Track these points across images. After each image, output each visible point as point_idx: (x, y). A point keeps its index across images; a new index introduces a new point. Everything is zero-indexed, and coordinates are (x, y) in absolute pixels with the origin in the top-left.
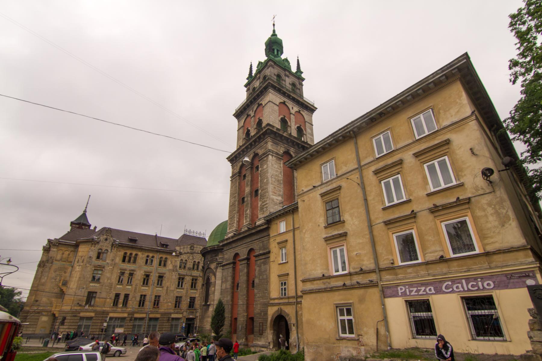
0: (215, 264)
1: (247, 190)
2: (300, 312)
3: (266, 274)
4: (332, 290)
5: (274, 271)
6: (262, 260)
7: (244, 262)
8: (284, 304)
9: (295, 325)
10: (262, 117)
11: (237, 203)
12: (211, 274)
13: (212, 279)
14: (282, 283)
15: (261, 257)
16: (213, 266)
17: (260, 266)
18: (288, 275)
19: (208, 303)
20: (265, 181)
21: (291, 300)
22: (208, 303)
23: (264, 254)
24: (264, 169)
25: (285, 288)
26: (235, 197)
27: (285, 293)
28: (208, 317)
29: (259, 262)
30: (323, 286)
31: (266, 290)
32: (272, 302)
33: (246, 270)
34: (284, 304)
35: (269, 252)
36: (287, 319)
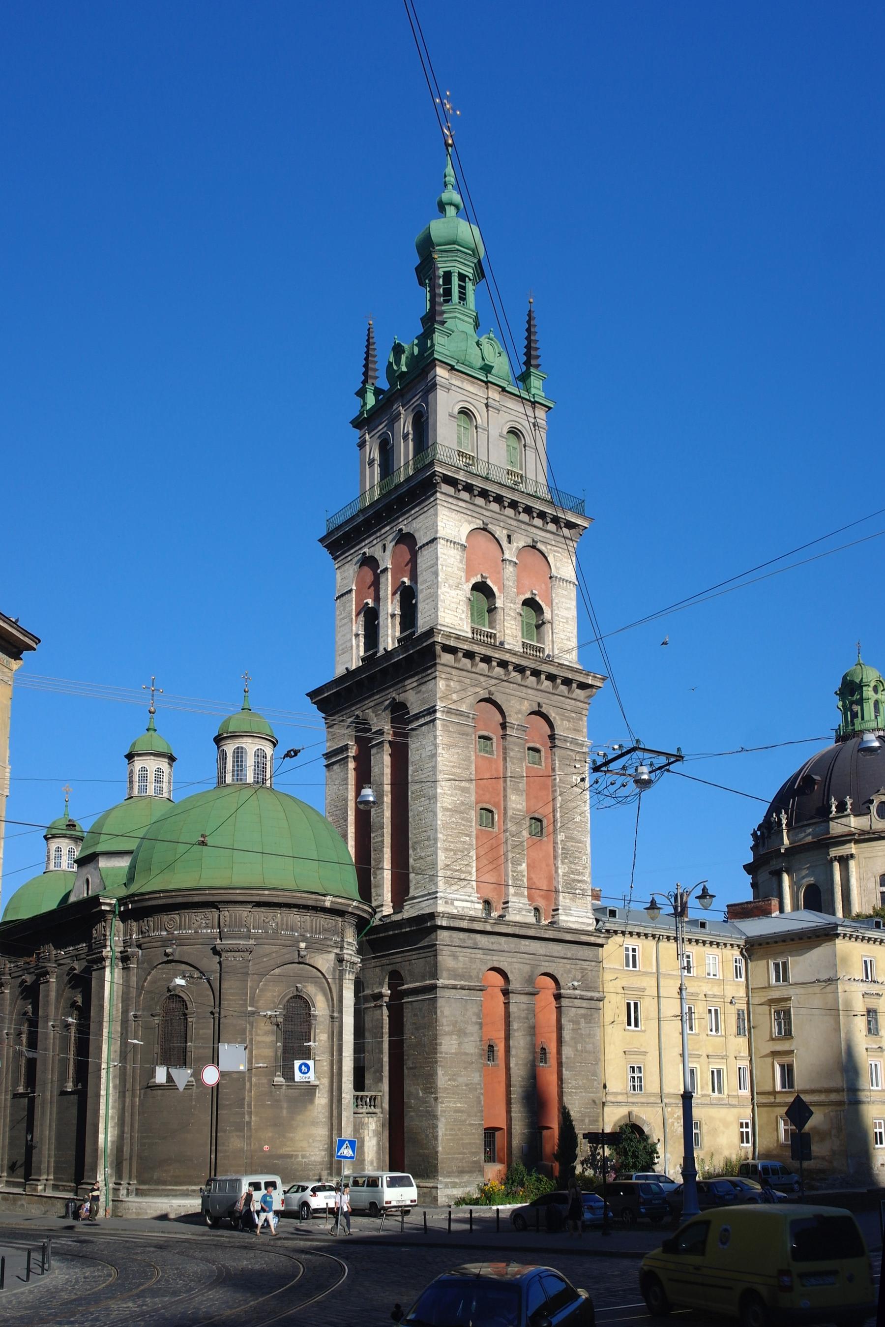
0: (332, 957)
1: (517, 803)
2: (670, 1120)
3: (593, 1044)
5: (616, 1041)
6: (583, 1011)
9: (662, 1139)
10: (551, 604)
11: (473, 813)
15: (577, 1002)
17: (576, 1022)
23: (591, 999)
25: (640, 1078)
27: (641, 1086)
31: (595, 1074)
36: (646, 1129)
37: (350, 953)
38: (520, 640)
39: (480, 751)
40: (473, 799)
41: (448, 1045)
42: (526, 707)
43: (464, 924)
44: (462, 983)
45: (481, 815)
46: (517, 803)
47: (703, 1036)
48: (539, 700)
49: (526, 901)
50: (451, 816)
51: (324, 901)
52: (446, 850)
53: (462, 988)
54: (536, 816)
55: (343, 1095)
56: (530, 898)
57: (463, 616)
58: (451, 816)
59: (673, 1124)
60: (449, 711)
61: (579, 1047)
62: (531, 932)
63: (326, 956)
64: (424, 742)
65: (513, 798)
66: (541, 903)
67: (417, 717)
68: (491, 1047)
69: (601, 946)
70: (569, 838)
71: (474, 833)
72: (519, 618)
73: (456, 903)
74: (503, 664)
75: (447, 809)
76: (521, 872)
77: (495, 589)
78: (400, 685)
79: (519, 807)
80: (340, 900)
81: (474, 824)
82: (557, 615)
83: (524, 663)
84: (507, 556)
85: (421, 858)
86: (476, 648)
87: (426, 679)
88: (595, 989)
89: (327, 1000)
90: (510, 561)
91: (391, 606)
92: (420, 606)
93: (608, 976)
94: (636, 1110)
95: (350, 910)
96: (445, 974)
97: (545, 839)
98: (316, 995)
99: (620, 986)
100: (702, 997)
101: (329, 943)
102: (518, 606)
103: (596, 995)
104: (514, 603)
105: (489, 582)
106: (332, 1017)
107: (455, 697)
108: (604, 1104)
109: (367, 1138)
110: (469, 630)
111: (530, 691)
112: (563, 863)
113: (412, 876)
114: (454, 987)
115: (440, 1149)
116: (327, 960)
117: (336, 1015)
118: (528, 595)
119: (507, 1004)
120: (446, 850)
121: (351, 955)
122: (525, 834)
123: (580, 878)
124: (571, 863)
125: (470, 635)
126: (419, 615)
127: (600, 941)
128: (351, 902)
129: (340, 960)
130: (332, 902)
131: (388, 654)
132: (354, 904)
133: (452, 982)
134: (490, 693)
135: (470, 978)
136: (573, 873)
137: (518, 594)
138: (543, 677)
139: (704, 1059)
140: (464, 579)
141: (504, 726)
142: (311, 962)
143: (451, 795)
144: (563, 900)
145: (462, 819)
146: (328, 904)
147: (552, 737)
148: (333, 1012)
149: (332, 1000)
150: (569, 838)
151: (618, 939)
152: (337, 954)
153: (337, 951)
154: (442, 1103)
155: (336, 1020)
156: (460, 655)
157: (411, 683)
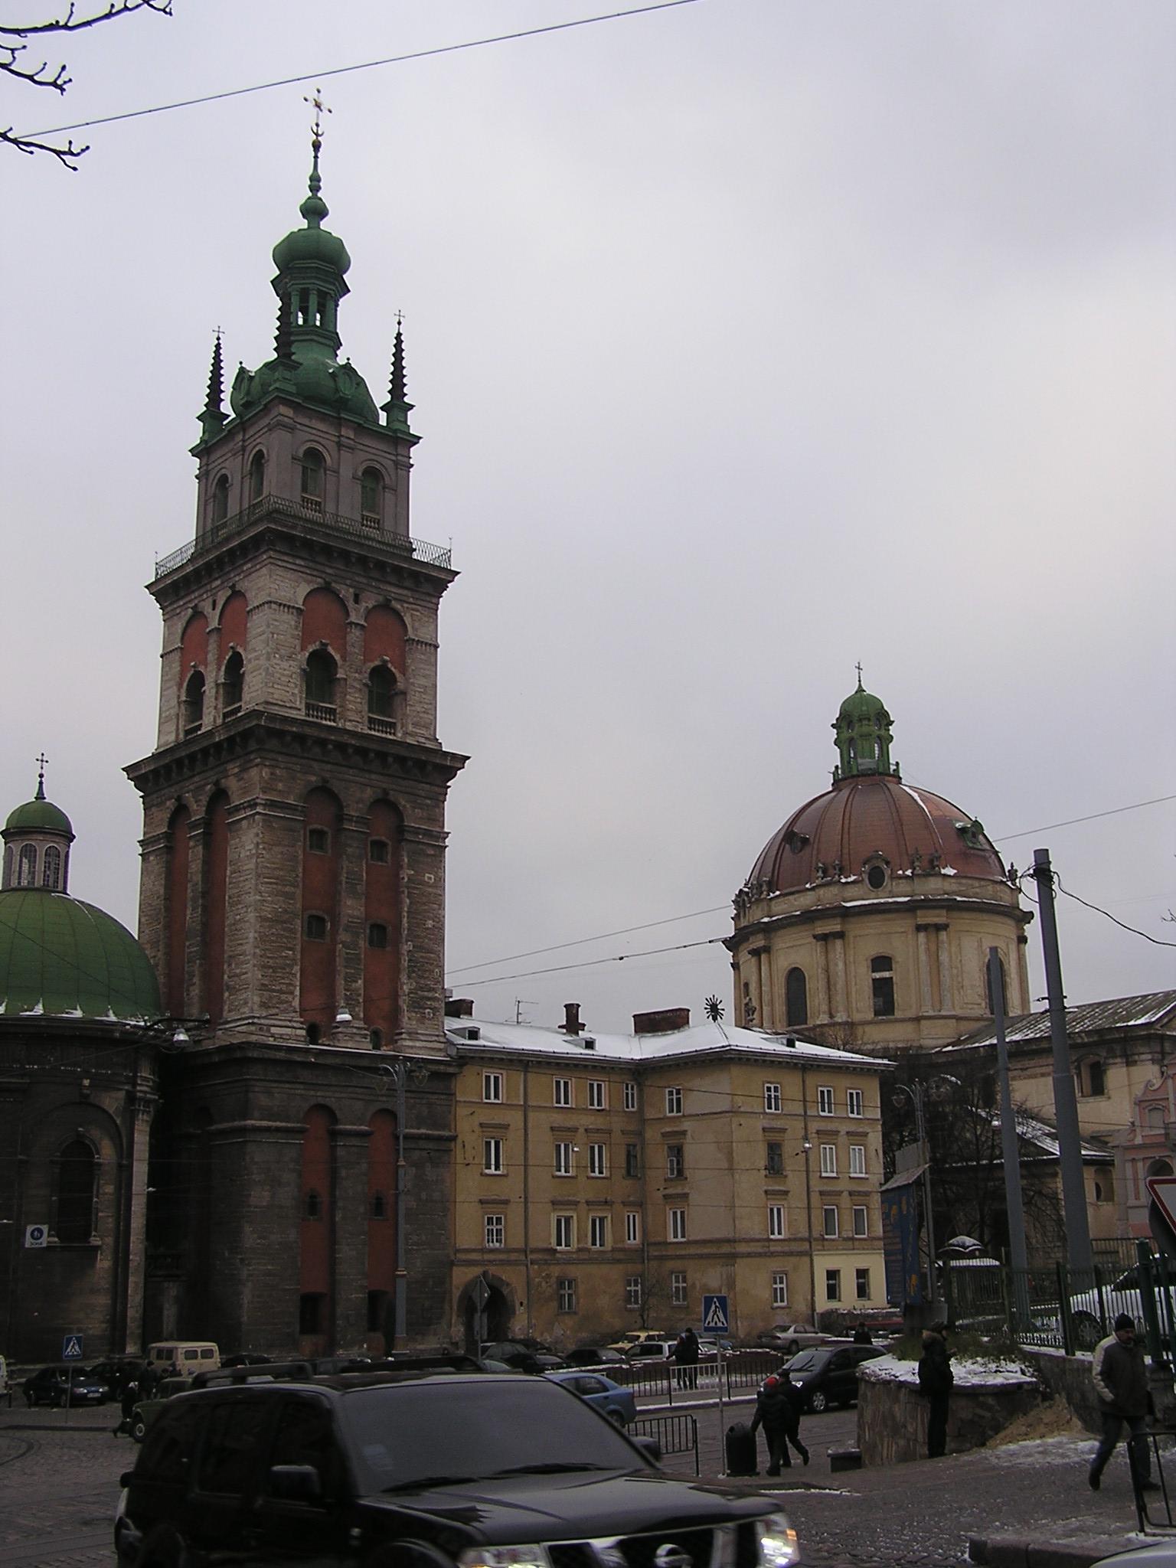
0: (122, 1095)
4: (772, 1254)
5: (468, 1186)
7: (355, 1141)
8: (503, 1263)
9: (525, 1302)
12: (95, 1133)
13: (107, 1153)
14: (490, 1221)
15: (422, 1144)
18: (506, 1202)
19: (95, 1241)
20: (430, 923)
21: (513, 1256)
22: (95, 1241)
23: (440, 1138)
24: (423, 883)
25: (499, 1232)
26: (286, 895)
29: (416, 1155)
30: (760, 1250)
32: (460, 1256)
33: (364, 1166)
34: (503, 1263)
35: (454, 1138)
37: (143, 1089)
38: (366, 714)
39: (311, 847)
40: (299, 906)
41: (259, 1196)
42: (369, 794)
43: (281, 1055)
44: (278, 1124)
45: (309, 923)
46: (352, 908)
47: (582, 1179)
48: (384, 786)
49: (361, 1024)
50: (270, 927)
51: (112, 1031)
52: (264, 967)
53: (278, 1129)
54: (379, 922)
56: (366, 1020)
57: (296, 691)
58: (270, 927)
59: (540, 1284)
60: (271, 804)
61: (424, 1196)
62: (365, 1063)
63: (114, 1094)
64: (244, 838)
65: (349, 903)
66: (381, 1026)
67: (237, 809)
68: (313, 1197)
69: (453, 1075)
70: (419, 948)
71: (298, 948)
72: (366, 690)
73: (273, 1030)
74: (341, 747)
75: (266, 919)
76: (358, 989)
77: (337, 657)
78: (221, 768)
79: (356, 913)
81: (299, 935)
82: (413, 684)
83: (365, 744)
84: (353, 618)
85: (236, 975)
86: (308, 731)
88: (444, 1127)
90: (357, 625)
91: (214, 676)
92: (247, 678)
93: (462, 1111)
94: (493, 1270)
96: (256, 1114)
97: (388, 949)
99: (477, 1123)
100: (581, 1130)
102: (365, 678)
103: (446, 1133)
104: (360, 673)
105: (330, 649)
106: (120, 1166)
107: (280, 786)
108: (452, 1264)
109: (167, 1306)
110: (303, 707)
111: (373, 776)
112: (409, 977)
113: (226, 994)
114: (268, 1129)
115: (245, 1319)
118: (377, 663)
119: (333, 1148)
120: (264, 967)
121: (145, 1092)
122: (362, 943)
123: (430, 995)
124: (420, 977)
125: (301, 715)
126: (246, 688)
127: (451, 1070)
129: (131, 1098)
131: (210, 733)
133: (265, 1123)
134: (325, 781)
135: (287, 1119)
136: (422, 989)
137: (365, 661)
138: (390, 759)
139: (583, 1207)
140: (298, 648)
141: (340, 818)
143: (272, 902)
144: (408, 1021)
145: (284, 930)
147: (400, 831)
149: (121, 1145)
150: (419, 948)
151: (476, 1069)
152: (128, 1091)
154: (249, 1265)
155: (125, 1170)
156: (289, 738)
157: (233, 768)
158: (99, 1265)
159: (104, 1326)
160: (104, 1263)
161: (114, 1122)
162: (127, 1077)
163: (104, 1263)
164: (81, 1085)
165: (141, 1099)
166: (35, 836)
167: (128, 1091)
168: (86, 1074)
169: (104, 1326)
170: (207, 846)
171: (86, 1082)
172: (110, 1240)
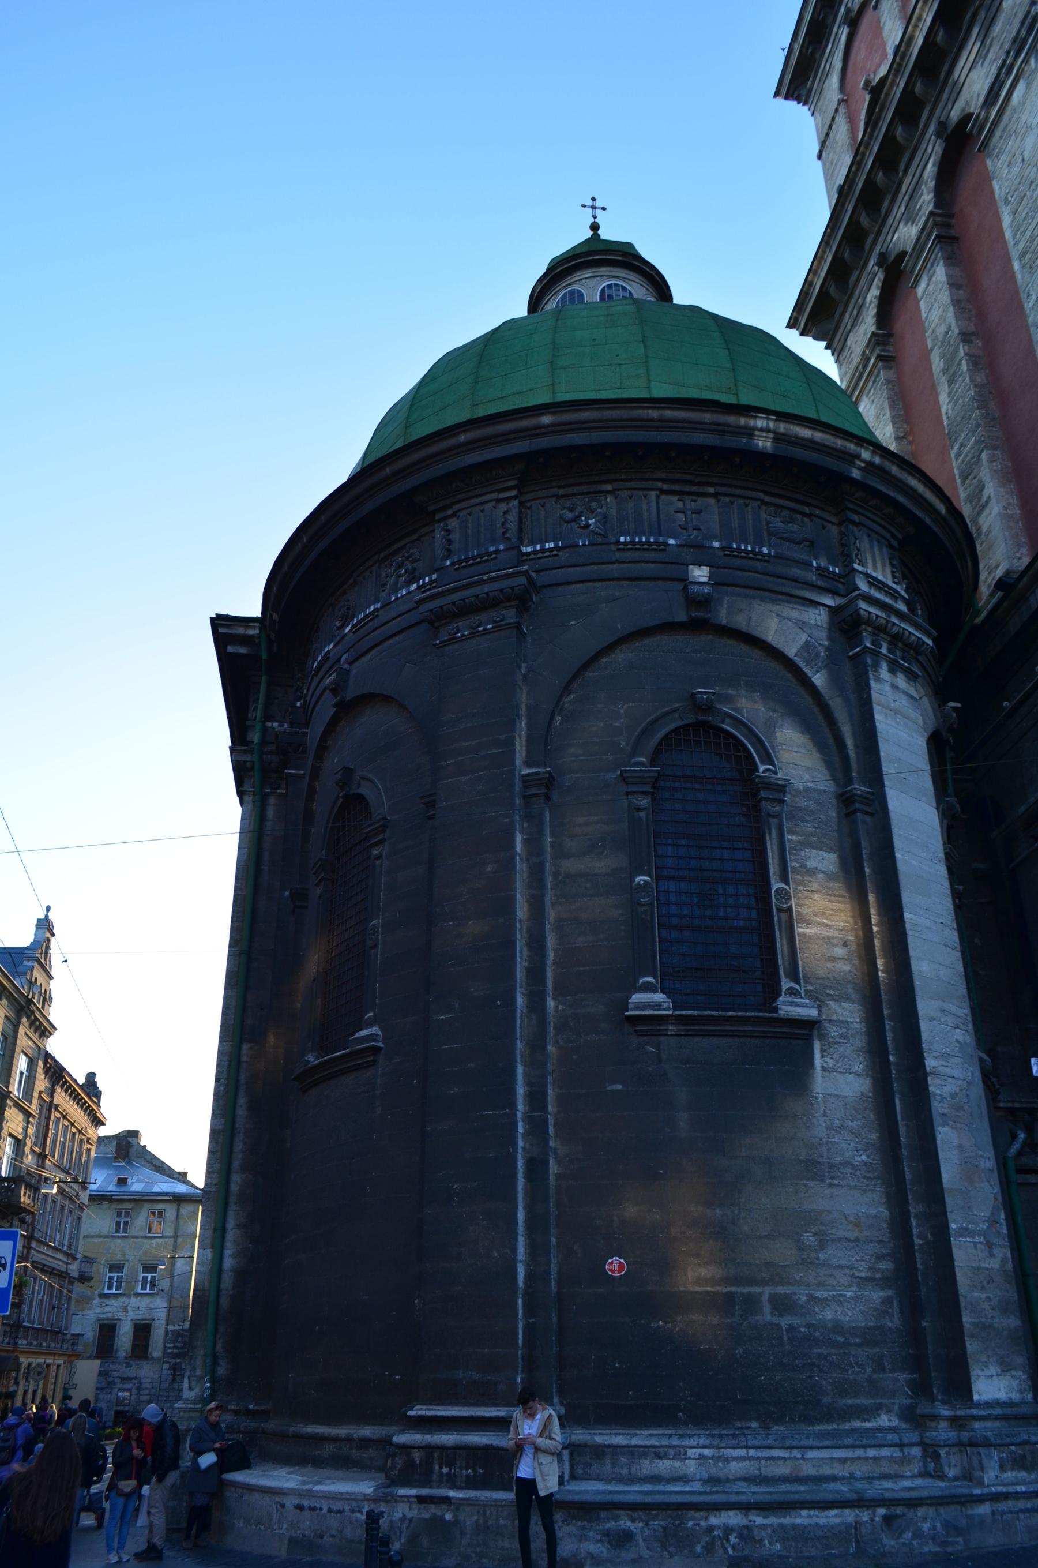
0: (818, 617)
12: (750, 707)
13: (795, 759)
16: (793, 628)
28: (815, 1169)
55: (930, 1063)
63: (794, 612)
80: (806, 433)
87: (994, 10)
89: (821, 747)
95: (856, 474)
98: (771, 726)
101: (797, 572)
106: (846, 801)
116: (802, 625)
117: (858, 788)
128: (851, 447)
129: (846, 625)
130: (779, 438)
132: (866, 455)
142: (740, 622)
146: (764, 443)
148: (850, 781)
152: (833, 611)
153: (829, 601)
158: (820, 1084)
159: (877, 1295)
160: (839, 1080)
161: (805, 681)
162: (822, 572)
163: (839, 1080)
164: (685, 580)
165: (880, 629)
166: (577, 276)
167: (833, 611)
168: (702, 555)
169: (877, 1295)
170: (951, 260)
171: (700, 573)
172: (847, 1013)
